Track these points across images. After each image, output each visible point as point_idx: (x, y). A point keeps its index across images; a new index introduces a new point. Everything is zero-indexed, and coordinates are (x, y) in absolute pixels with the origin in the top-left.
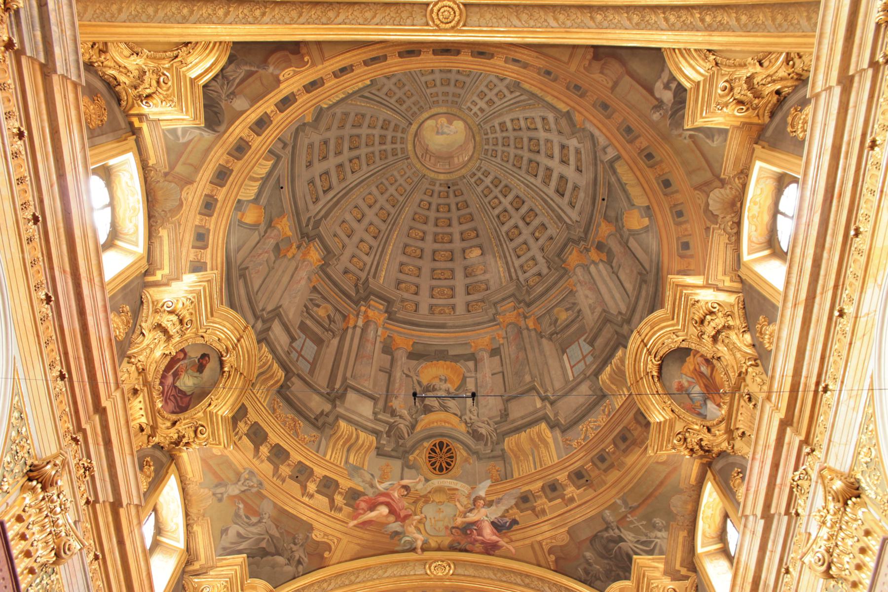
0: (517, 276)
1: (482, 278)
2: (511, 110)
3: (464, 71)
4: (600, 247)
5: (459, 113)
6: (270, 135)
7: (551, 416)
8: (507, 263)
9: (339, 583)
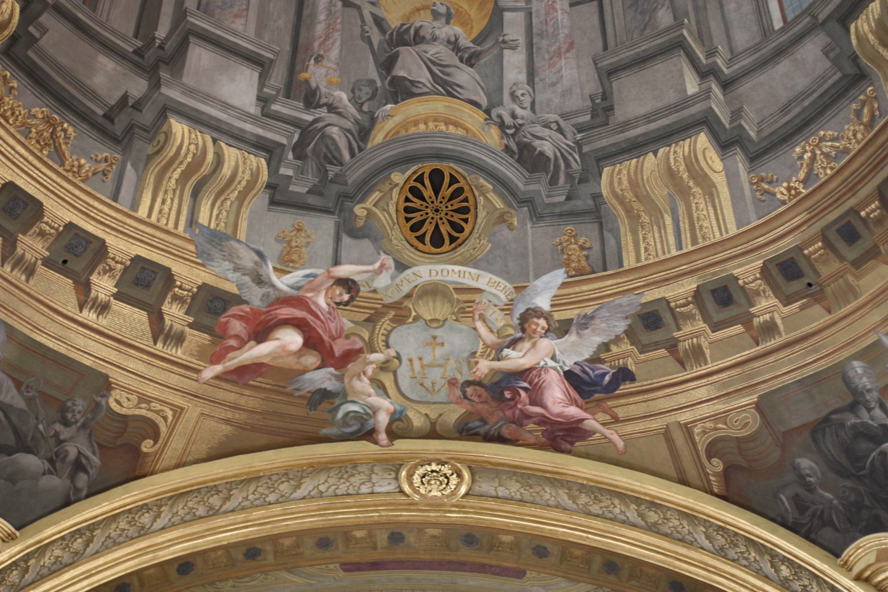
7: (723, 116)
9: (181, 512)
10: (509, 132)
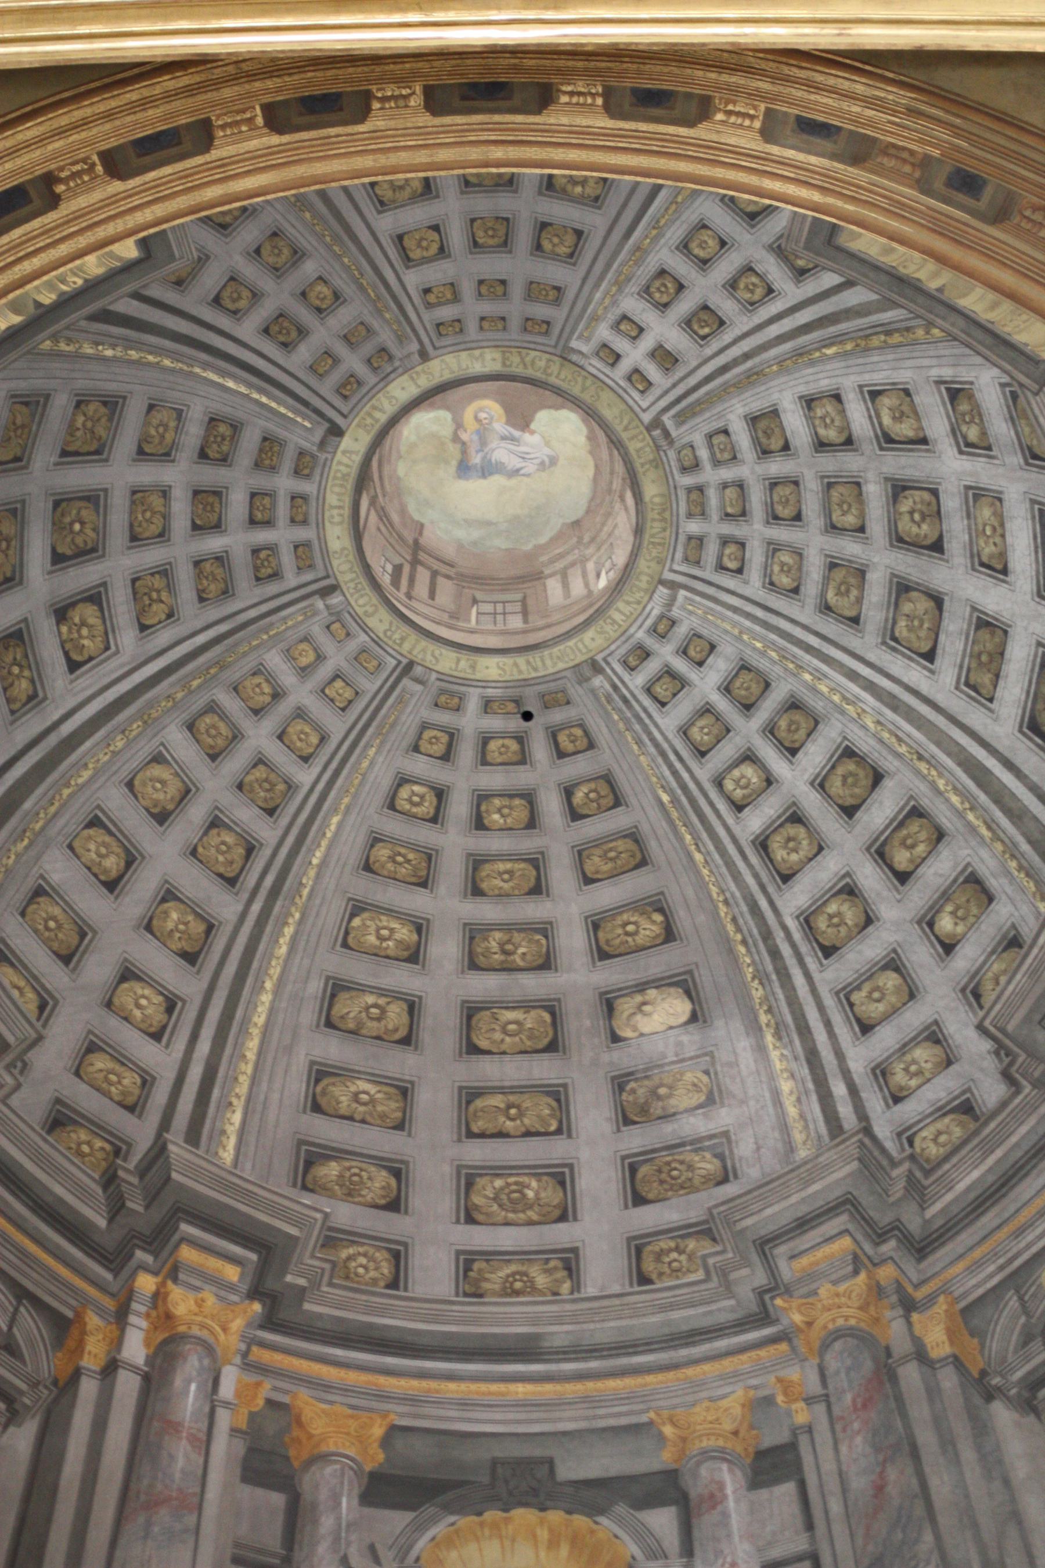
0: (862, 1115)
1: (696, 1125)
2: (799, 354)
3: (572, 181)
5: (559, 375)
8: (812, 1057)
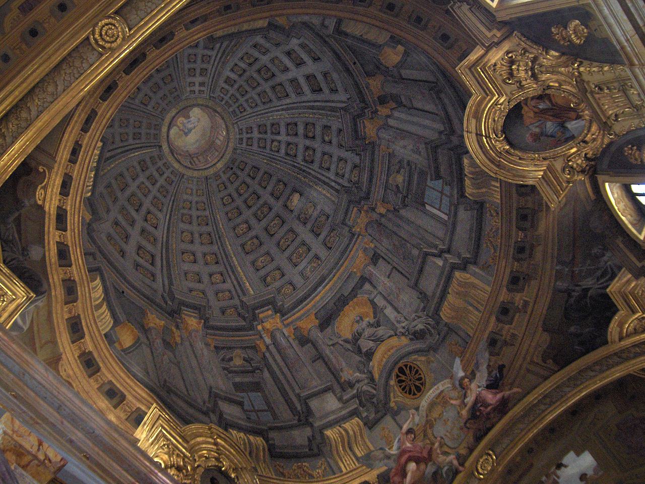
0: (339, 184)
1: (316, 214)
2: (223, 63)
4: (382, 100)
6: (76, 255)
7: (456, 261)
8: (324, 183)
10: (407, 334)
